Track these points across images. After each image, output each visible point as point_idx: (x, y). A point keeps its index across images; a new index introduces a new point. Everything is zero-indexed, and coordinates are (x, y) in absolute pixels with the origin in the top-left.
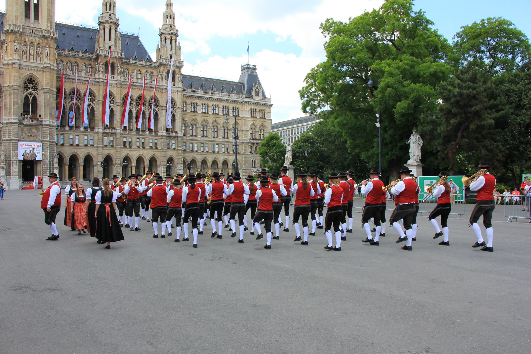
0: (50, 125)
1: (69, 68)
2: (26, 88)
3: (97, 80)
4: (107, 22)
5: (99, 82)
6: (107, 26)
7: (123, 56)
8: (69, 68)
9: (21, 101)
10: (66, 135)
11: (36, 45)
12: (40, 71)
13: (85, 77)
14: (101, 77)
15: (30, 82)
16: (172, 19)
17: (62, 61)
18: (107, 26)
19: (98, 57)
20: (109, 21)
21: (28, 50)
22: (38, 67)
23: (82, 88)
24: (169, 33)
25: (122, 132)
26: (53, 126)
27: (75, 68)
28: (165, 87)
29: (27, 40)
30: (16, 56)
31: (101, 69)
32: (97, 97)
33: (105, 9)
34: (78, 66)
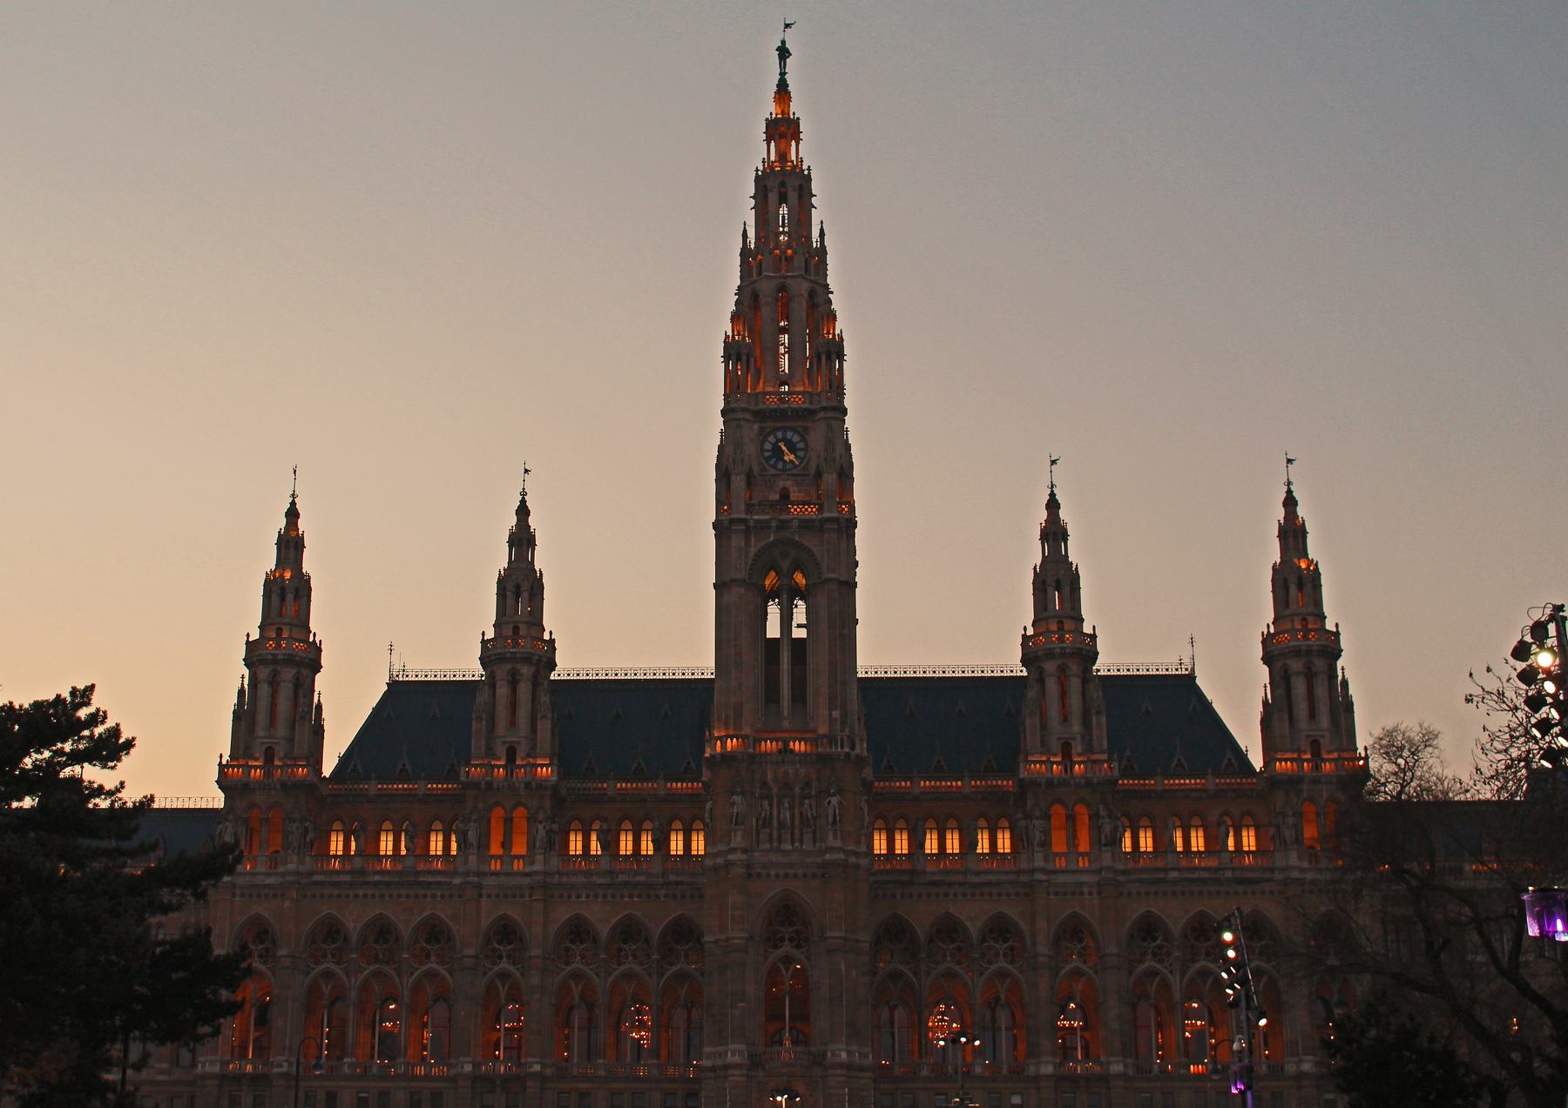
0: (849, 1067)
2: (774, 941)
3: (1023, 878)
4: (1050, 655)
7: (1116, 773)
11: (797, 790)
12: (814, 876)
13: (978, 873)
15: (787, 921)
16: (1308, 589)
18: (1050, 666)
19: (1023, 786)
23: (973, 916)
24: (1296, 652)
25: (1131, 1072)
26: (862, 1069)
28: (1296, 874)
30: (738, 840)
32: (1028, 943)
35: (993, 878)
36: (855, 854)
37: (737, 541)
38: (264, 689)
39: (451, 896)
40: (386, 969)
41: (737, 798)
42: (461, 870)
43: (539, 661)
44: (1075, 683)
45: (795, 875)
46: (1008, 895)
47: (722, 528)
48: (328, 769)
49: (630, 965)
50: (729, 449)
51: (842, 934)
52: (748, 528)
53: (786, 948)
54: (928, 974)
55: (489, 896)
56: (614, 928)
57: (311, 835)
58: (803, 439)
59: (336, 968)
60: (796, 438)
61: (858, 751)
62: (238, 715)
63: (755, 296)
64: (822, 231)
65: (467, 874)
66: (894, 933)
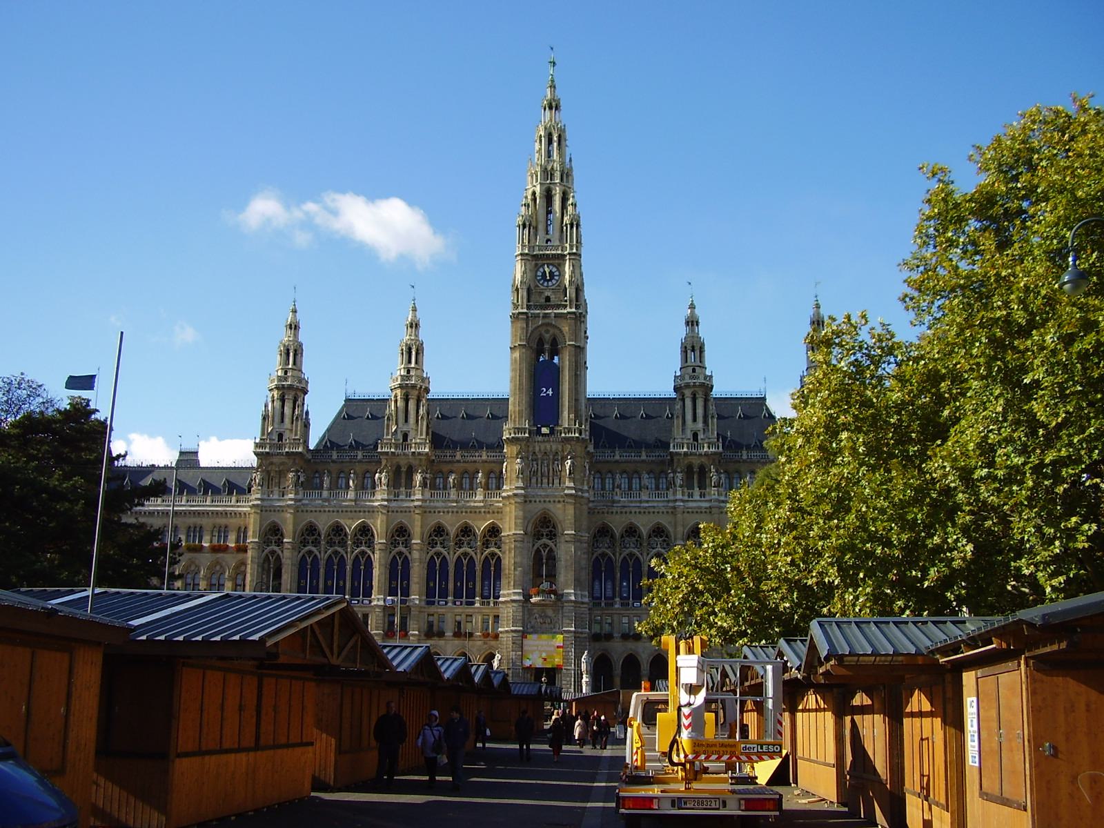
0: (575, 602)
1: (619, 487)
4: (687, 386)
5: (674, 508)
6: (688, 393)
7: (721, 449)
8: (619, 487)
9: (528, 562)
10: (616, 618)
11: (551, 457)
12: (559, 502)
13: (647, 502)
14: (679, 496)
17: (610, 472)
18: (688, 393)
20: (693, 384)
21: (539, 467)
22: (556, 496)
23: (644, 525)
26: (583, 603)
27: (635, 482)
29: (537, 449)
31: (679, 482)
33: (684, 361)
34: (640, 478)
35: (655, 504)
36: (581, 490)
37: (521, 324)
38: (278, 404)
39: (373, 512)
40: (339, 549)
41: (518, 460)
42: (379, 498)
43: (421, 387)
44: (700, 403)
45: (550, 501)
46: (663, 513)
47: (515, 317)
48: (312, 447)
49: (465, 549)
50: (519, 277)
51: (573, 532)
52: (528, 317)
53: (545, 540)
54: (620, 554)
55: (393, 512)
56: (458, 529)
57: (302, 479)
58: (558, 270)
59: (314, 549)
60: (554, 270)
61: (583, 436)
62: (264, 419)
63: (534, 193)
64: (570, 159)
65: (383, 500)
66: (604, 532)
